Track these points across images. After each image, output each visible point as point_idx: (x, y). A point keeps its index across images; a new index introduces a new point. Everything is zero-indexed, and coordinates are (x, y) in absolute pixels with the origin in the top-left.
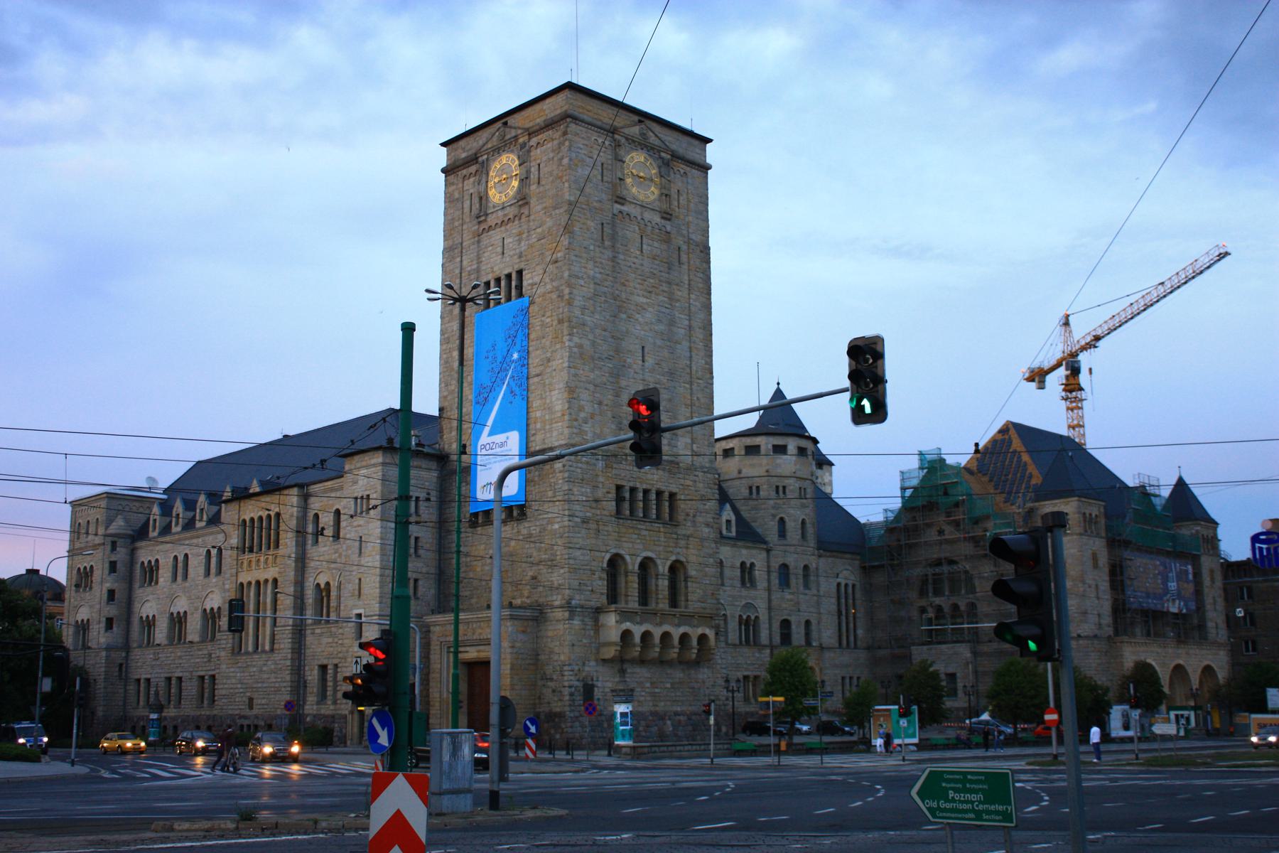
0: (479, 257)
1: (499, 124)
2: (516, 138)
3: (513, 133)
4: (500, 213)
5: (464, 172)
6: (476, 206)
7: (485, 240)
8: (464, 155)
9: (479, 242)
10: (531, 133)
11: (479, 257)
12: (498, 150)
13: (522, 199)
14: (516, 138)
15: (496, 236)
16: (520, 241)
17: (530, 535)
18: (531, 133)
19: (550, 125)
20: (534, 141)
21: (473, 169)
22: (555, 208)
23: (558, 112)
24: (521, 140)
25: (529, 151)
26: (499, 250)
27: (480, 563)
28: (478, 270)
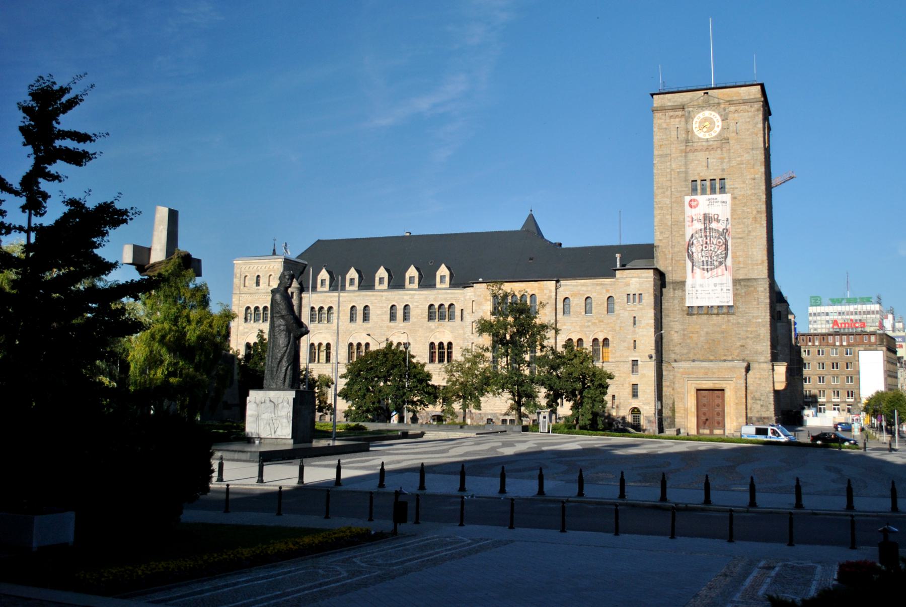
0: (686, 164)
1: (702, 92)
2: (719, 104)
3: (716, 101)
4: (704, 143)
5: (672, 114)
6: (683, 136)
7: (691, 156)
8: (669, 104)
9: (686, 156)
10: (730, 103)
11: (686, 164)
12: (701, 107)
13: (723, 140)
14: (719, 104)
15: (702, 156)
16: (722, 163)
17: (738, 323)
18: (730, 103)
19: (745, 102)
20: (733, 108)
21: (680, 113)
22: (753, 149)
23: (752, 97)
24: (722, 106)
25: (728, 113)
26: (705, 164)
27: (695, 335)
28: (686, 172)
